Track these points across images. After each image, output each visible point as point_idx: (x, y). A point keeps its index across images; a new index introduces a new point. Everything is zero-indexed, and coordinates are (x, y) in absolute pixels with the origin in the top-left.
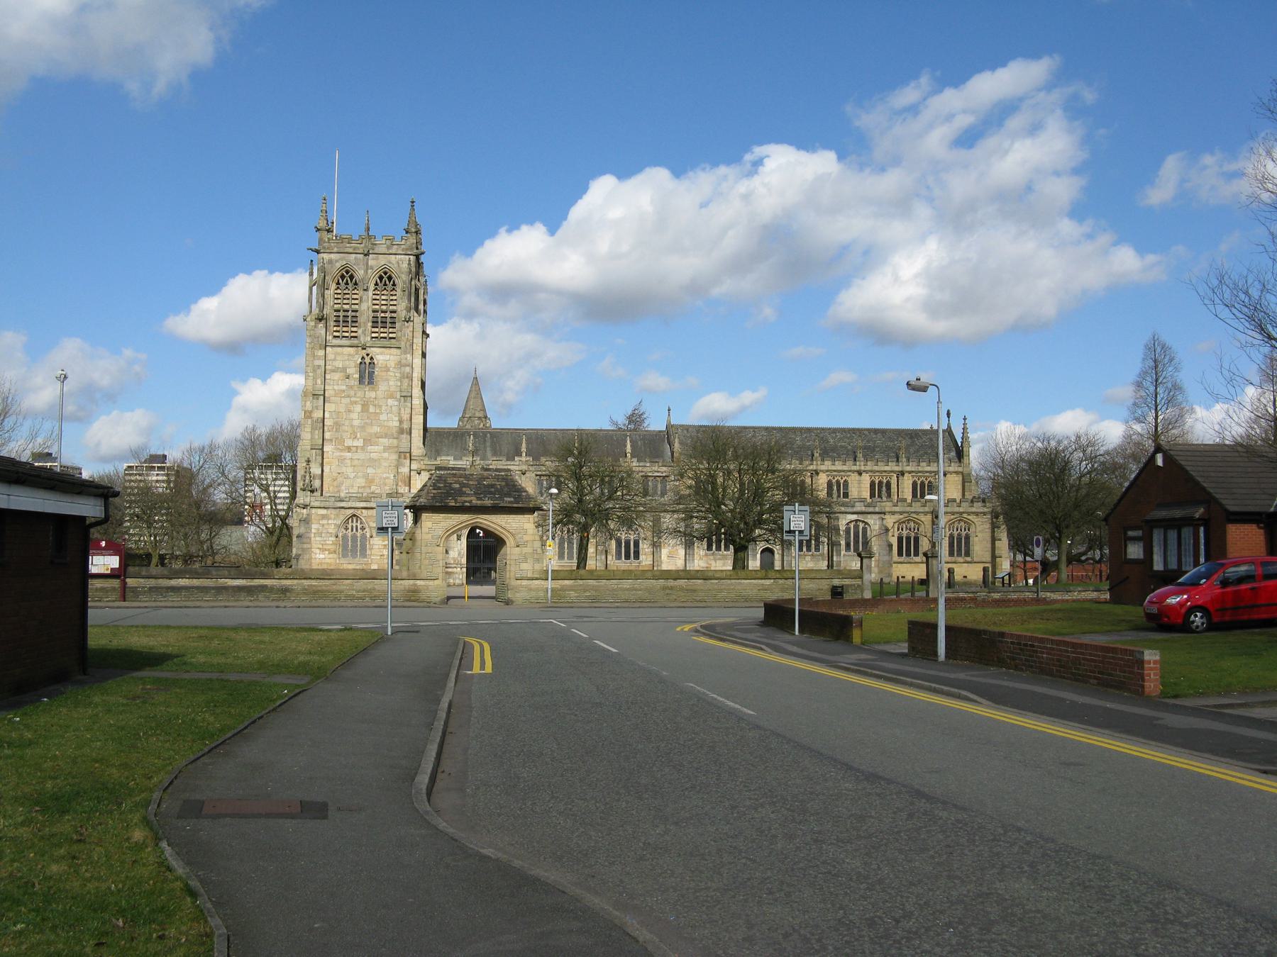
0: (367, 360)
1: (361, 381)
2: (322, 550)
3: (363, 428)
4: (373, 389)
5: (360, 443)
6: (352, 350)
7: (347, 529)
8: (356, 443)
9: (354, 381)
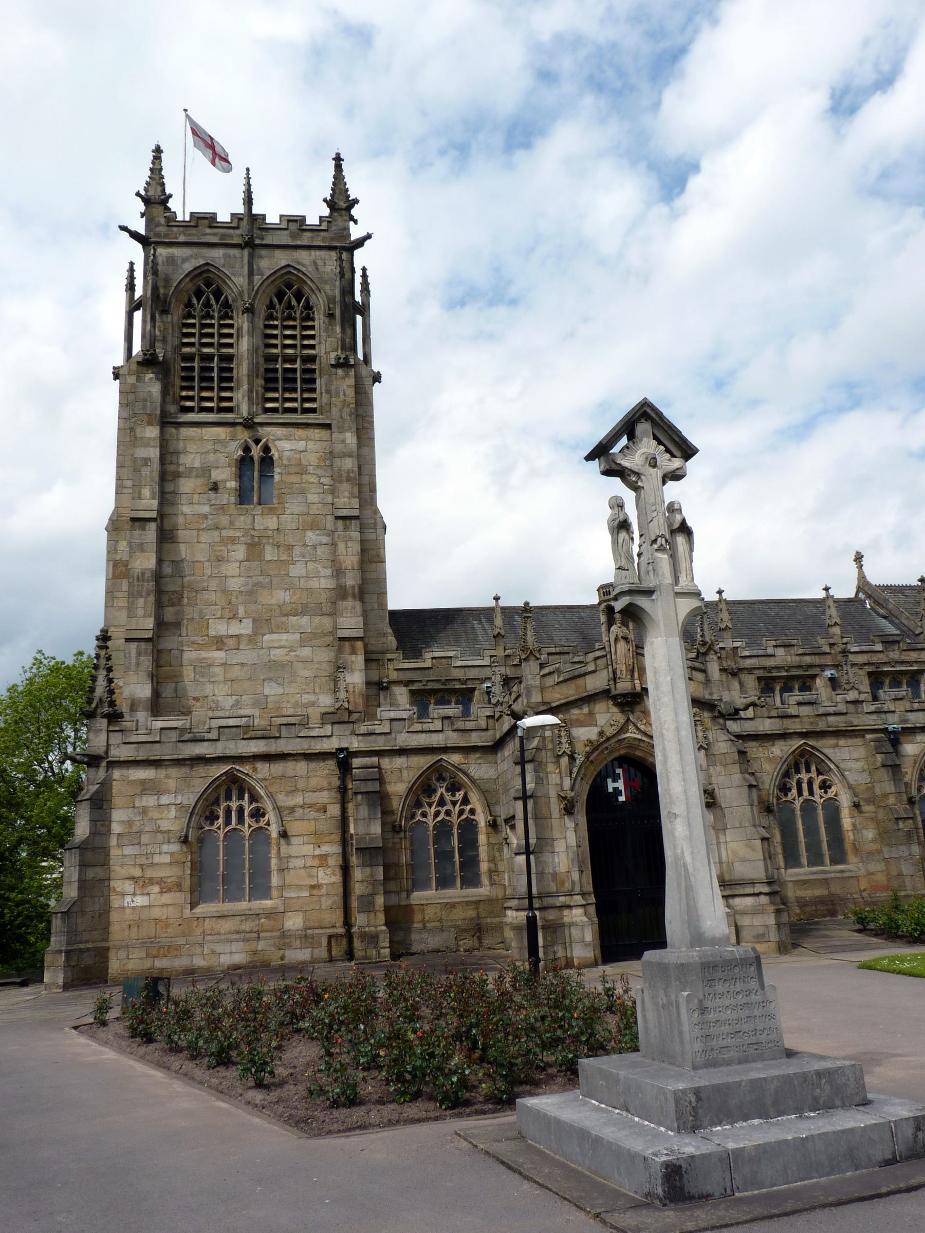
0: (256, 452)
1: (243, 496)
2: (142, 883)
3: (251, 594)
4: (272, 511)
5: (245, 628)
6: (221, 432)
7: (213, 818)
8: (235, 629)
9: (227, 497)
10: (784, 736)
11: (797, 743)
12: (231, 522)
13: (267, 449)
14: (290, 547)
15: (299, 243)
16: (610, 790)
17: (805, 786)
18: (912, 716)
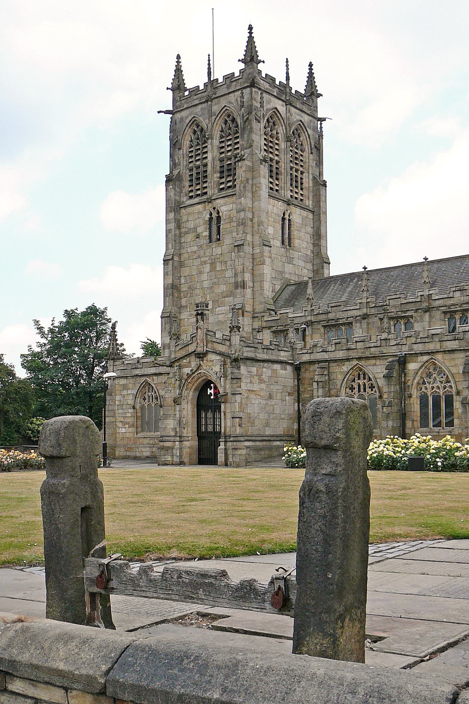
0: (214, 215)
4: (219, 245)
6: (200, 207)
10: (348, 360)
11: (355, 362)
12: (204, 254)
13: (218, 213)
14: (226, 262)
15: (231, 90)
16: (209, 394)
17: (362, 387)
18: (415, 347)
